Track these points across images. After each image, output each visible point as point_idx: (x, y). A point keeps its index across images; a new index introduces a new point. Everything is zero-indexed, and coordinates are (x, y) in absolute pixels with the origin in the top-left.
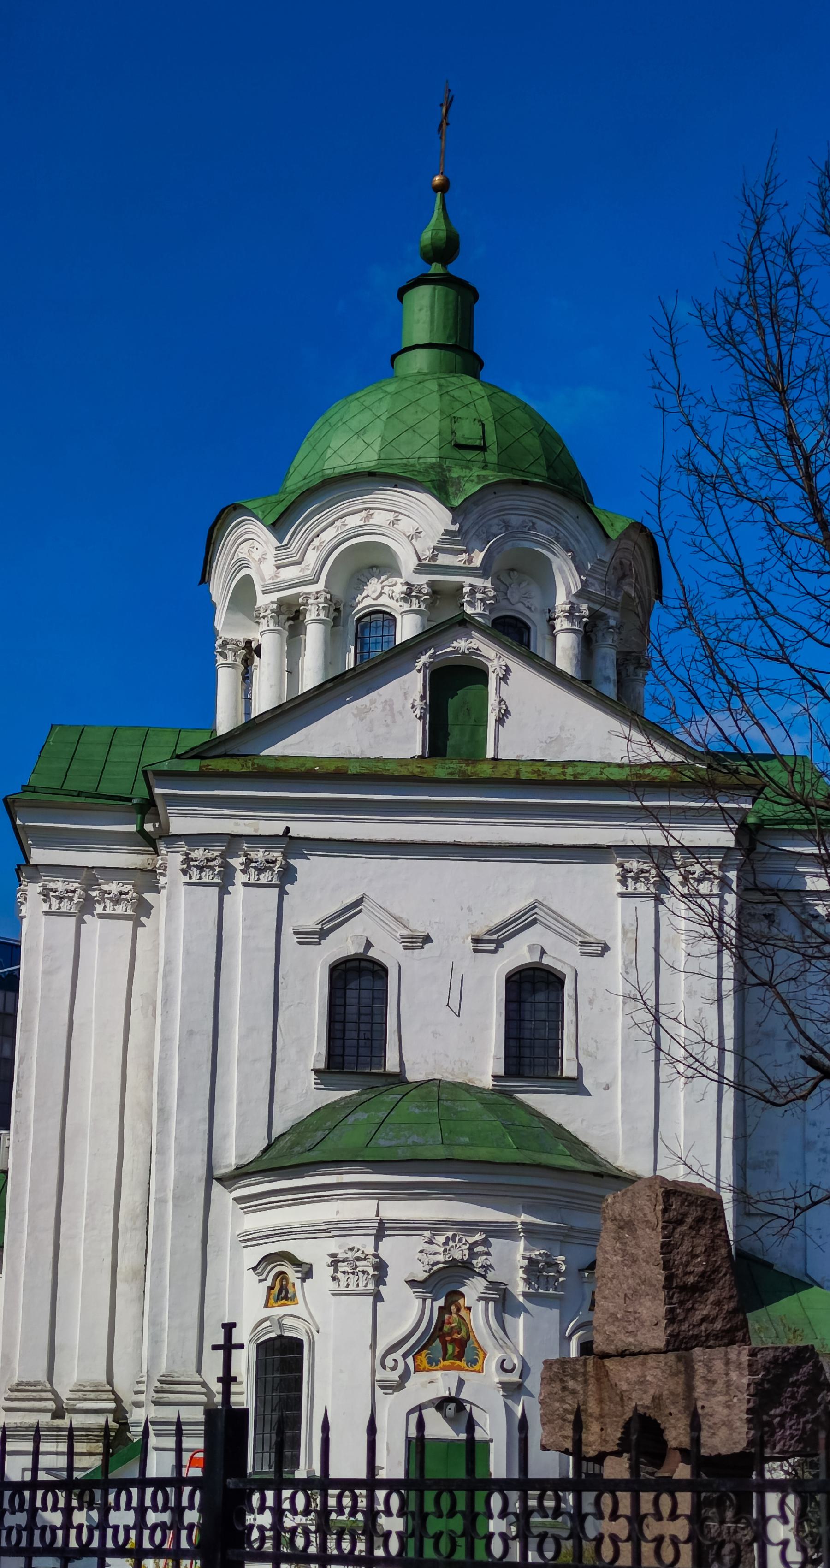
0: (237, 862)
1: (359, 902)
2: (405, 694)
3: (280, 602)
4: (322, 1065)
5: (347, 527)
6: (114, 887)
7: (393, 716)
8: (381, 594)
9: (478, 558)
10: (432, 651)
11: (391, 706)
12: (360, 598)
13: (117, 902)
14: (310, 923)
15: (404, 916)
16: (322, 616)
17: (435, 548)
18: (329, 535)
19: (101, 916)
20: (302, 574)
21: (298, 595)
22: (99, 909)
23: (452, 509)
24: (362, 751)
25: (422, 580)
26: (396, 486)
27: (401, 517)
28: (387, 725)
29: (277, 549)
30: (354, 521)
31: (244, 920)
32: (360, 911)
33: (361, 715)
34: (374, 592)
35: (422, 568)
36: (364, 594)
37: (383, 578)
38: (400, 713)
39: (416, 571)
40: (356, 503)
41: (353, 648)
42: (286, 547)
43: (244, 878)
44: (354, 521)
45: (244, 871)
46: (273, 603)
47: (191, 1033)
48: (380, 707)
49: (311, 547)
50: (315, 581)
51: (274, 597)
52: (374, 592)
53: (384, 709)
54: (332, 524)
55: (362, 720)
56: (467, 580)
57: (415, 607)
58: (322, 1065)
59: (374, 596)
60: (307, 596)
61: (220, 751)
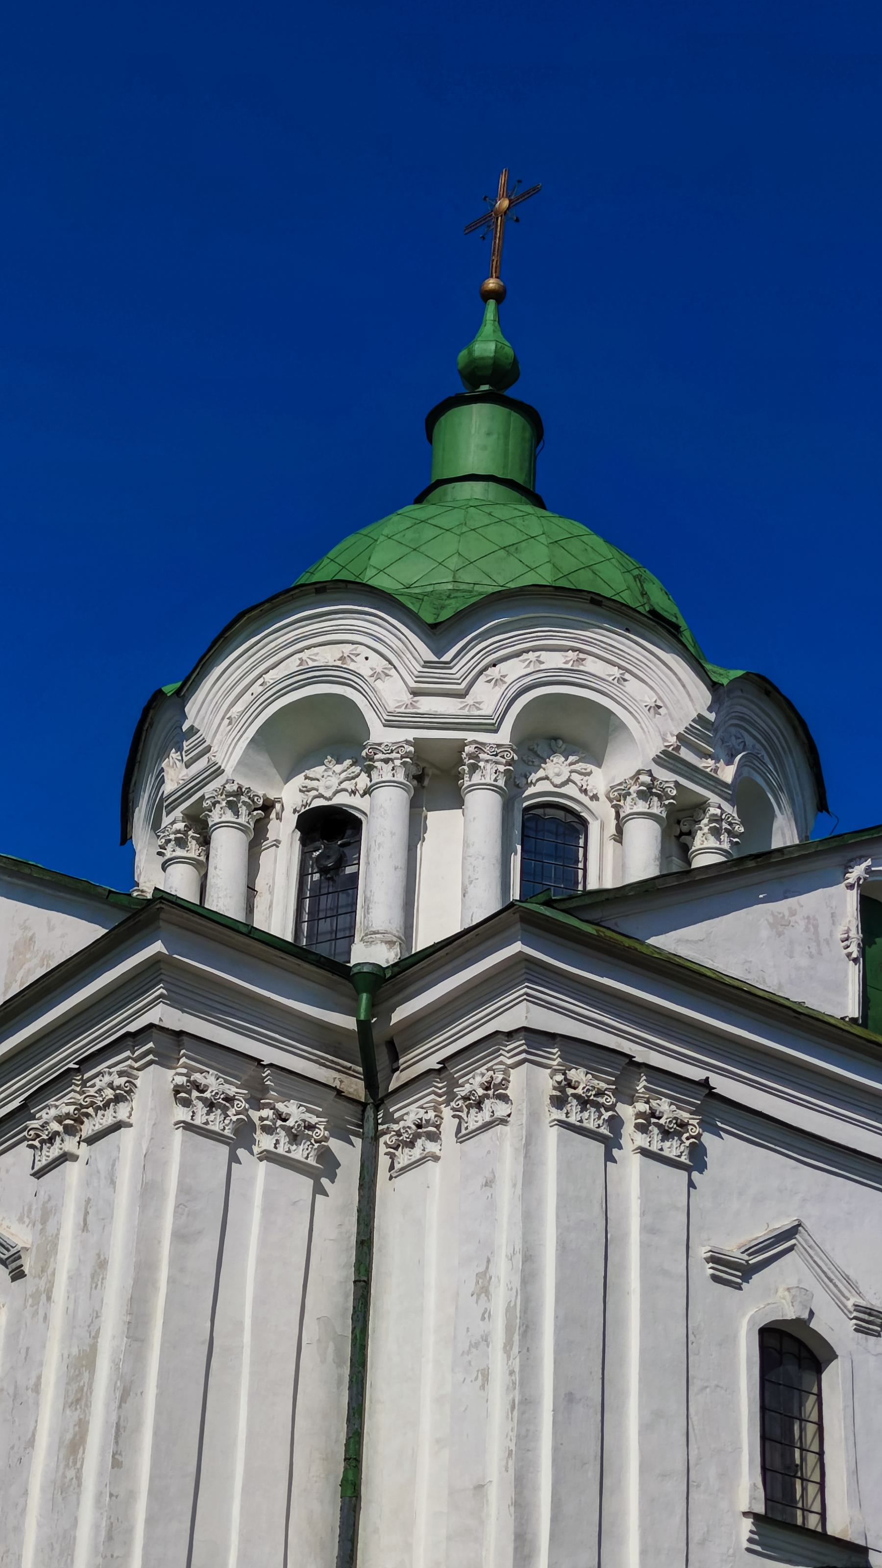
0: (627, 1112)
1: (791, 1233)
2: (833, 915)
3: (417, 743)
4: (760, 1509)
5: (543, 667)
6: (295, 1112)
7: (818, 945)
8: (569, 780)
9: (728, 773)
10: (869, 862)
11: (816, 927)
12: (533, 777)
13: (295, 1138)
14: (733, 1247)
15: (851, 1273)
16: (501, 783)
17: (679, 737)
18: (514, 670)
19: (268, 1156)
20: (465, 712)
21: (463, 744)
22: (265, 1142)
23: (713, 686)
24: (780, 986)
25: (664, 776)
26: (627, 630)
27: (627, 676)
28: (811, 956)
29: (427, 664)
30: (554, 660)
31: (643, 1214)
32: (791, 1249)
33: (780, 925)
34: (558, 775)
35: (668, 758)
36: (541, 773)
37: (571, 758)
38: (828, 943)
39: (657, 760)
40: (562, 636)
41: (519, 847)
42: (447, 665)
43: (641, 1140)
44: (554, 660)
45: (643, 1129)
46: (407, 742)
47: (570, 1398)
48: (802, 924)
49: (482, 678)
50: (494, 729)
51: (411, 734)
52: (558, 775)
53: (807, 929)
54: (518, 654)
55: (780, 934)
56: (714, 798)
57: (656, 809)
58: (760, 1509)
59: (558, 781)
60: (480, 746)
61: (596, 915)
